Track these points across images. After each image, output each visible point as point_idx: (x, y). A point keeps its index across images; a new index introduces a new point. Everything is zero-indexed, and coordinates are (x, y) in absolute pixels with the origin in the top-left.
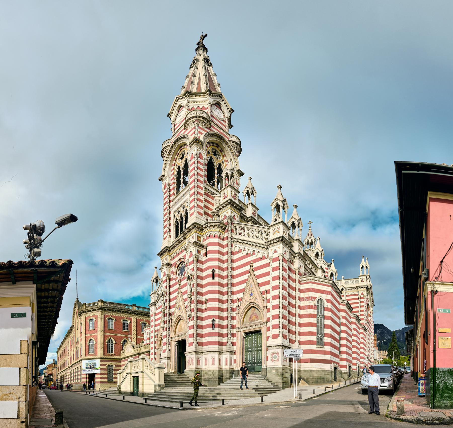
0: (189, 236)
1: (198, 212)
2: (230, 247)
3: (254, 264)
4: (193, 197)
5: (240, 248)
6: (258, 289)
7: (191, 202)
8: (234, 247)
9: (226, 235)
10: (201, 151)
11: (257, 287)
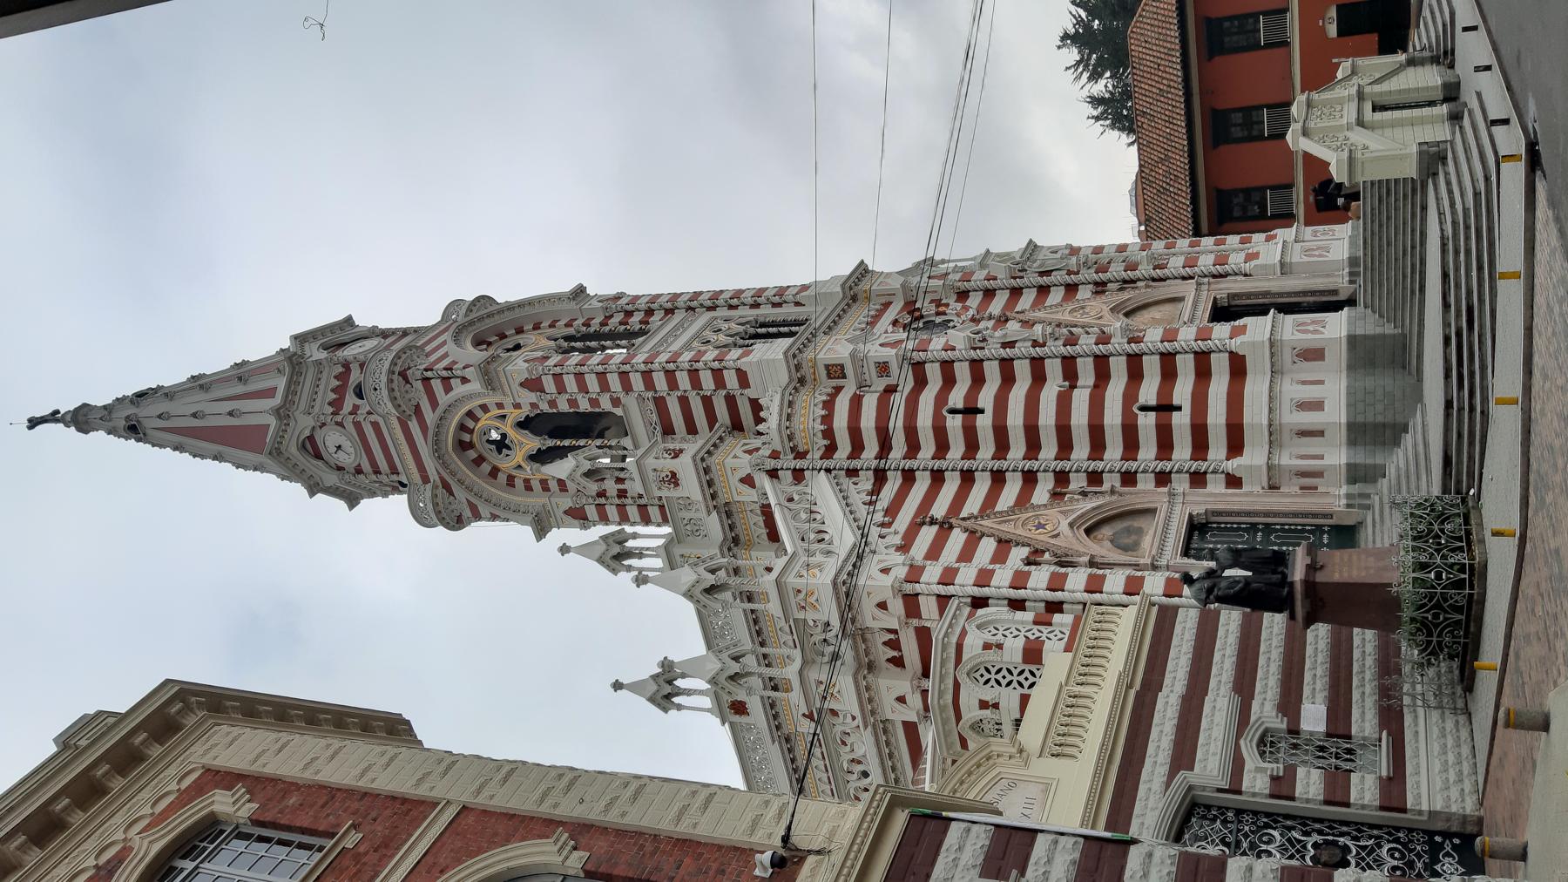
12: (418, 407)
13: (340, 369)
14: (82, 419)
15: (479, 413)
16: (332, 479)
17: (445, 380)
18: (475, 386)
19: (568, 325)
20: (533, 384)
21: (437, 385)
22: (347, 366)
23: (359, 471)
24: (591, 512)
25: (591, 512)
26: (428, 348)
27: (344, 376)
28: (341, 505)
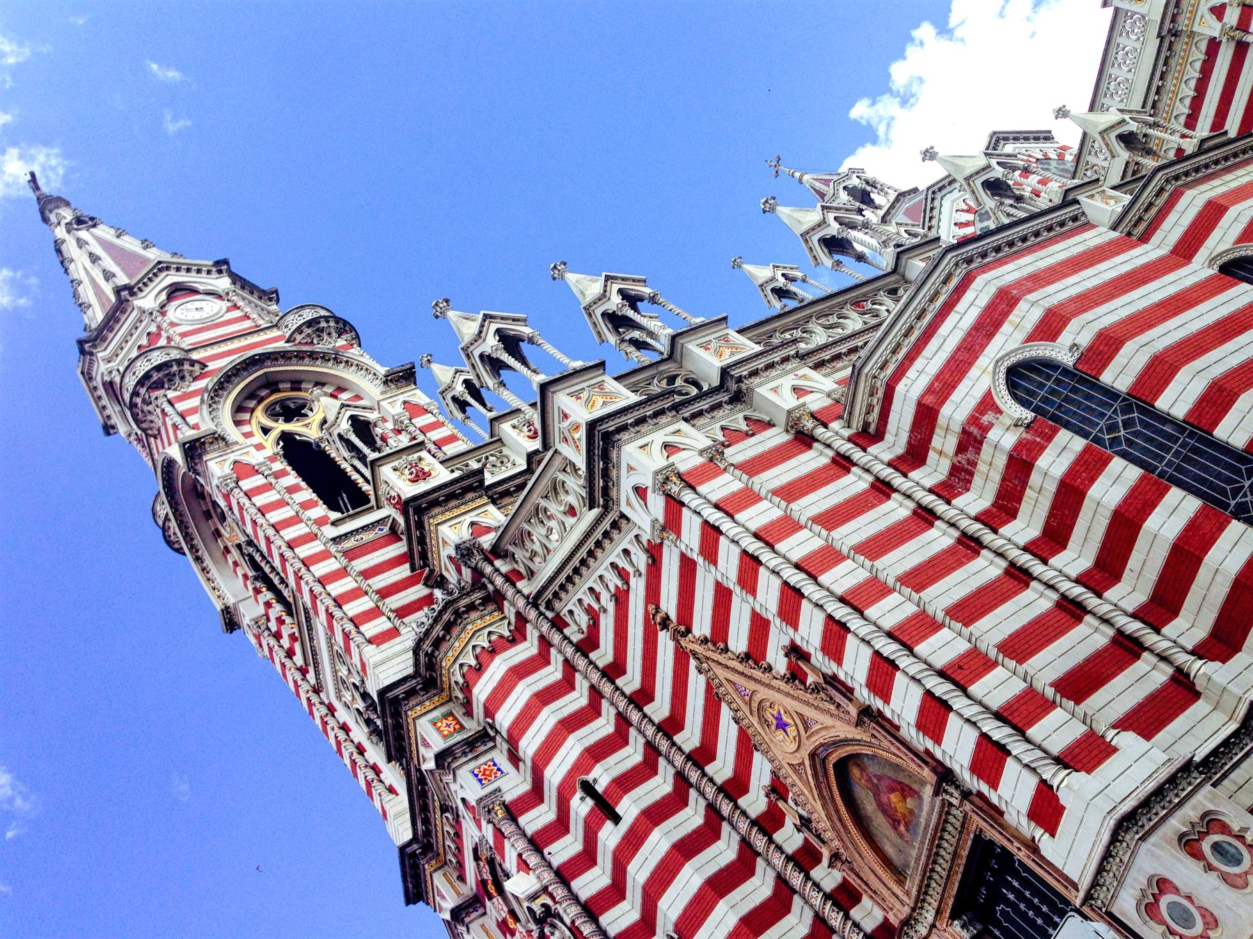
1: (370, 641)
3: (663, 606)
6: (765, 678)
8: (568, 619)
9: (510, 611)
10: (232, 457)
11: (757, 674)
13: (153, 329)
26: (212, 366)
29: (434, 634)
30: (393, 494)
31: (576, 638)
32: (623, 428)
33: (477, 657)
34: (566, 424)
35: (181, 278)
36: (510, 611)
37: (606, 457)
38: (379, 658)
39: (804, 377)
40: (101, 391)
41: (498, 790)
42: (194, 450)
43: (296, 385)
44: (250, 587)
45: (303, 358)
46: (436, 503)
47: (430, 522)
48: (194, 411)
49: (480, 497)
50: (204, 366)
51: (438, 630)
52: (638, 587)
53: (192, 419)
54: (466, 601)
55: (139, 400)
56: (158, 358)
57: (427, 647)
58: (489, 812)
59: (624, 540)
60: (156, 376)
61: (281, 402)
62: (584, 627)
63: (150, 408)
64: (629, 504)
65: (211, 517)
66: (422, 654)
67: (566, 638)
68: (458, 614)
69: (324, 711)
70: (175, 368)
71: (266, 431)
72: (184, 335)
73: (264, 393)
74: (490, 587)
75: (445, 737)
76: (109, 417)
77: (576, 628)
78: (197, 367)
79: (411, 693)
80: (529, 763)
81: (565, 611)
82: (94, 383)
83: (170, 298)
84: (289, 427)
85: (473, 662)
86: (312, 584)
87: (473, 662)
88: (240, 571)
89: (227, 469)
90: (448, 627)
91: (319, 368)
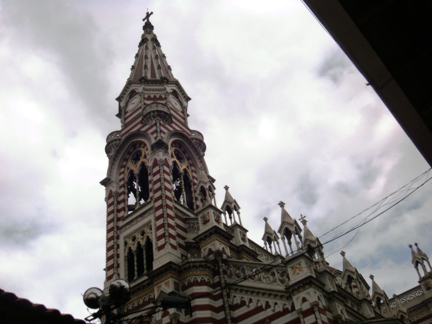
0: (159, 281)
1: (171, 244)
2: (226, 299)
4: (160, 222)
5: (243, 299)
7: (158, 228)
8: (232, 297)
9: (217, 279)
10: (166, 157)
12: (146, 125)
13: (163, 96)
14: (148, 27)
15: (146, 148)
16: (123, 104)
17: (156, 131)
18: (153, 141)
19: (194, 177)
20: (155, 164)
21: (154, 129)
22: (165, 98)
23: (126, 113)
24: (111, 200)
25: (111, 200)
26: (173, 125)
27: (161, 98)
28: (117, 112)
29: (196, 264)
30: (207, 217)
31: (230, 303)
32: (314, 284)
33: (201, 281)
34: (298, 266)
35: (178, 91)
36: (217, 279)
37: (304, 285)
38: (171, 251)
39: (343, 309)
40: (129, 91)
41: (179, 315)
42: (160, 145)
43: (185, 152)
44: (122, 183)
45: (193, 148)
46: (220, 234)
47: (214, 237)
48: (164, 133)
49: (228, 243)
50: (172, 123)
51: (198, 264)
52: (269, 312)
53: (163, 135)
54: (209, 265)
55: (152, 114)
56: (165, 110)
57: (191, 265)
58: (175, 318)
59: (280, 303)
60: (162, 114)
61: (179, 152)
62: (235, 303)
63: (153, 118)
64: (297, 298)
65: (130, 155)
66: (188, 265)
67: (228, 301)
68: (206, 265)
69: (115, 235)
70: (168, 117)
71: (172, 156)
72: (171, 108)
73: (178, 145)
74: (217, 268)
75: (175, 289)
76: (123, 97)
77: (232, 301)
78: (171, 122)
79: (175, 270)
80: (194, 318)
81: (233, 295)
82: (130, 87)
83: (171, 93)
84: (178, 162)
85: (199, 281)
86: (165, 213)
87: (199, 281)
88: (122, 176)
89: (163, 158)
90: (201, 266)
91: (194, 154)
